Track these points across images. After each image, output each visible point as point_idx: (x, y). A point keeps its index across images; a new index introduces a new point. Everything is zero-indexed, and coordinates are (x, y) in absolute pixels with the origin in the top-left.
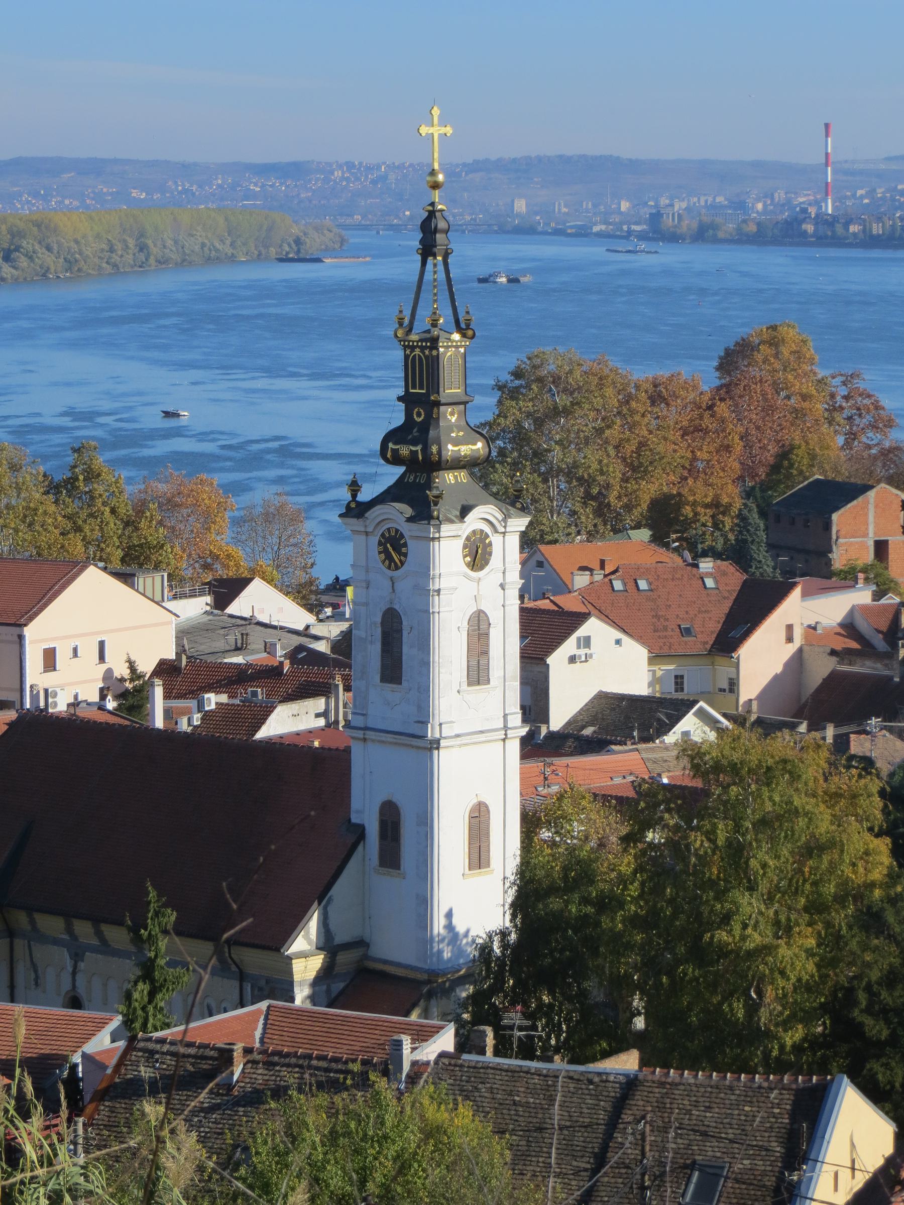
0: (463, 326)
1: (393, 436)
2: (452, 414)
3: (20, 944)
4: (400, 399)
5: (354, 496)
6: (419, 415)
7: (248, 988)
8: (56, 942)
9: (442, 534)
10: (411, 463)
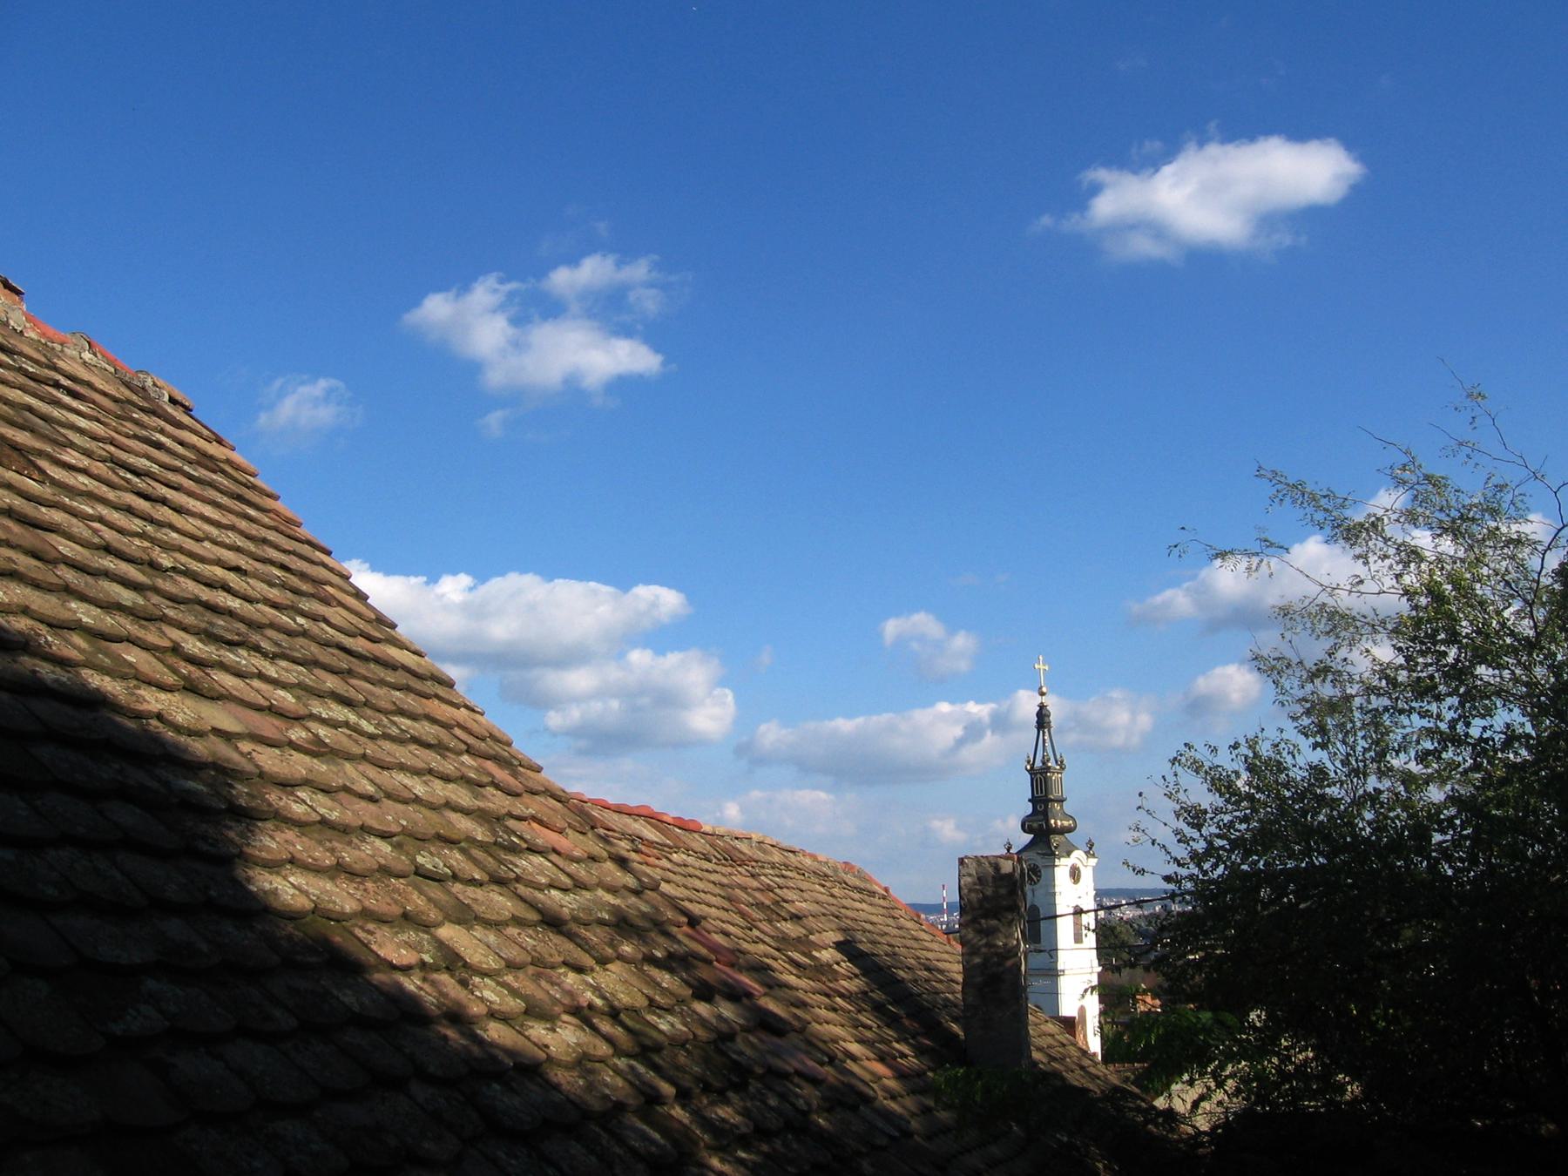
4: (1030, 800)
5: (1008, 850)
6: (1041, 807)
9: (1061, 863)
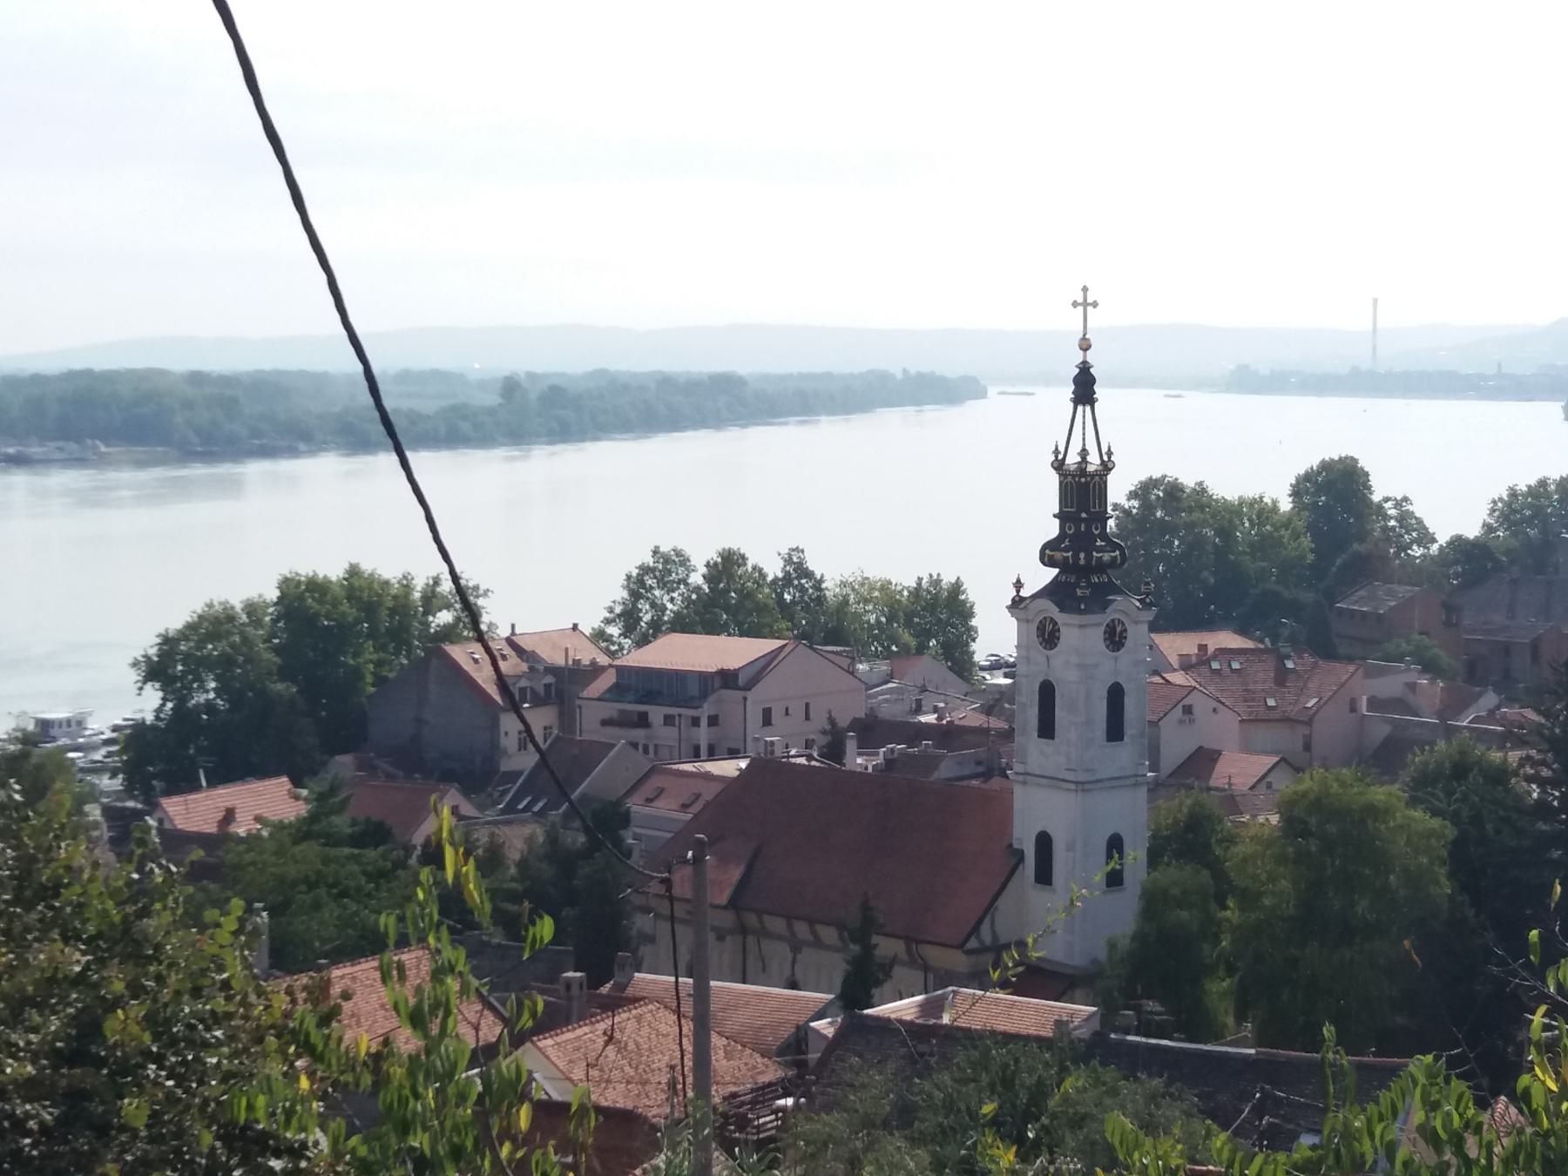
0: (1105, 458)
1: (1048, 546)
2: (1097, 529)
3: (751, 940)
4: (1055, 516)
5: (1018, 591)
7: (931, 976)
8: (780, 938)
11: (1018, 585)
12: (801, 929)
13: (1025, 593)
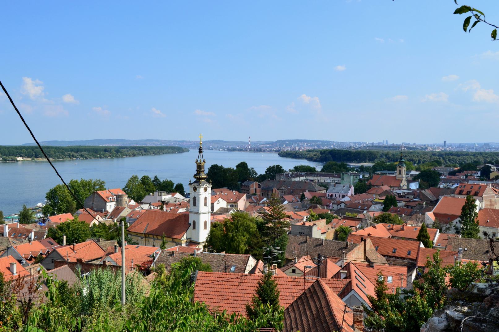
8: (151, 238)
10: (198, 178)
11: (190, 181)
12: (155, 237)
13: (191, 183)
